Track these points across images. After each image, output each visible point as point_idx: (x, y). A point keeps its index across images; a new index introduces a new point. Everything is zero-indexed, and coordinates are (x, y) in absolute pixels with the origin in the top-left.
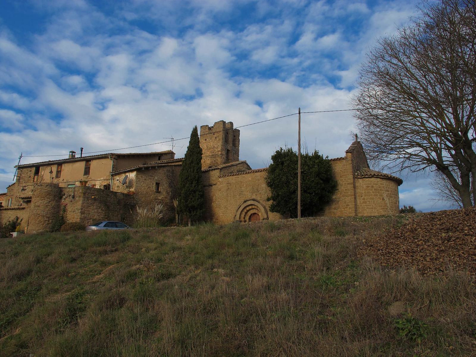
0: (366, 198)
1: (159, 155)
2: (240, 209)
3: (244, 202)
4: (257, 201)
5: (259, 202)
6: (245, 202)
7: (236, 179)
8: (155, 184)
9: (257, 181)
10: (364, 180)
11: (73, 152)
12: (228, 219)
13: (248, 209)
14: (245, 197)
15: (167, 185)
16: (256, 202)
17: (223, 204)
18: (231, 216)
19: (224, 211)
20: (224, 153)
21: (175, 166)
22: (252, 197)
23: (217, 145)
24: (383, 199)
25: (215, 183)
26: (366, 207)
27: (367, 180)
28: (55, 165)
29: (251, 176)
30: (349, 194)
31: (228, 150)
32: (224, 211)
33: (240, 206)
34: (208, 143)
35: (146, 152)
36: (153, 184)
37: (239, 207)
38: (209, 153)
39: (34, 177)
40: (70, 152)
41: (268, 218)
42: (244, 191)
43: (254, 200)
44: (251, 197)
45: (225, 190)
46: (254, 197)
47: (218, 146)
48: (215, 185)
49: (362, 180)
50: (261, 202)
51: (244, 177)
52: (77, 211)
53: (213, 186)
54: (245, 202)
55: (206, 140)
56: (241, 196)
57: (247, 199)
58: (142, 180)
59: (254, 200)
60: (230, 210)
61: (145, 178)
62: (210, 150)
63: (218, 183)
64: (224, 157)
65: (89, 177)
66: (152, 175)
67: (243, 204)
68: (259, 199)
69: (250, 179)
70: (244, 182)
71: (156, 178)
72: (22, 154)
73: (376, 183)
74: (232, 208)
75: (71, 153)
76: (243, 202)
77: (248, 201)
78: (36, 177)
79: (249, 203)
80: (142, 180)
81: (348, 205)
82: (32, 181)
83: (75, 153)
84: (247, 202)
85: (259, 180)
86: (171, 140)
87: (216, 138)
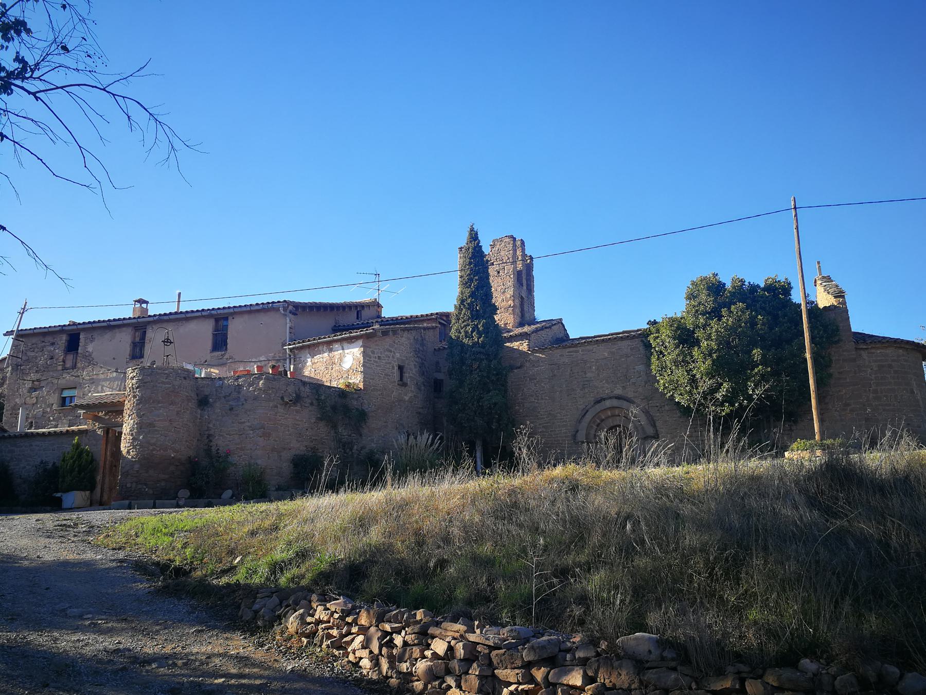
0: (879, 390)
1: (358, 308)
2: (587, 416)
3: (595, 403)
4: (625, 400)
6: (598, 402)
7: (571, 355)
8: (396, 368)
9: (623, 359)
10: (871, 353)
11: (141, 301)
12: (559, 439)
14: (596, 391)
15: (417, 369)
16: (625, 402)
17: (543, 409)
18: (566, 433)
19: (545, 423)
20: (517, 302)
21: (425, 329)
22: (615, 392)
24: (912, 392)
25: (519, 365)
26: (880, 407)
27: (879, 352)
28: (124, 329)
29: (608, 348)
30: (848, 380)
31: (522, 298)
32: (545, 423)
33: (587, 411)
35: (330, 301)
36: (393, 367)
37: (586, 413)
39: (65, 357)
40: (135, 301)
41: (658, 435)
42: (592, 379)
43: (619, 398)
44: (612, 392)
45: (546, 378)
46: (618, 391)
48: (519, 368)
49: (869, 353)
52: (251, 432)
53: (515, 371)
54: (598, 402)
56: (587, 391)
57: (602, 396)
58: (374, 359)
59: (619, 398)
60: (561, 419)
61: (380, 355)
63: (528, 364)
64: (518, 310)
66: (390, 349)
67: (592, 406)
68: (630, 395)
69: (606, 354)
70: (593, 360)
71: (398, 355)
72: (26, 303)
73: (895, 358)
74: (567, 415)
75: (138, 305)
76: (592, 404)
77: (604, 399)
78: (70, 357)
79: (608, 403)
80: (374, 359)
81: (848, 405)
82: (60, 368)
83: (147, 302)
84: (603, 402)
85: (627, 356)
86: (373, 278)
87: (499, 272)
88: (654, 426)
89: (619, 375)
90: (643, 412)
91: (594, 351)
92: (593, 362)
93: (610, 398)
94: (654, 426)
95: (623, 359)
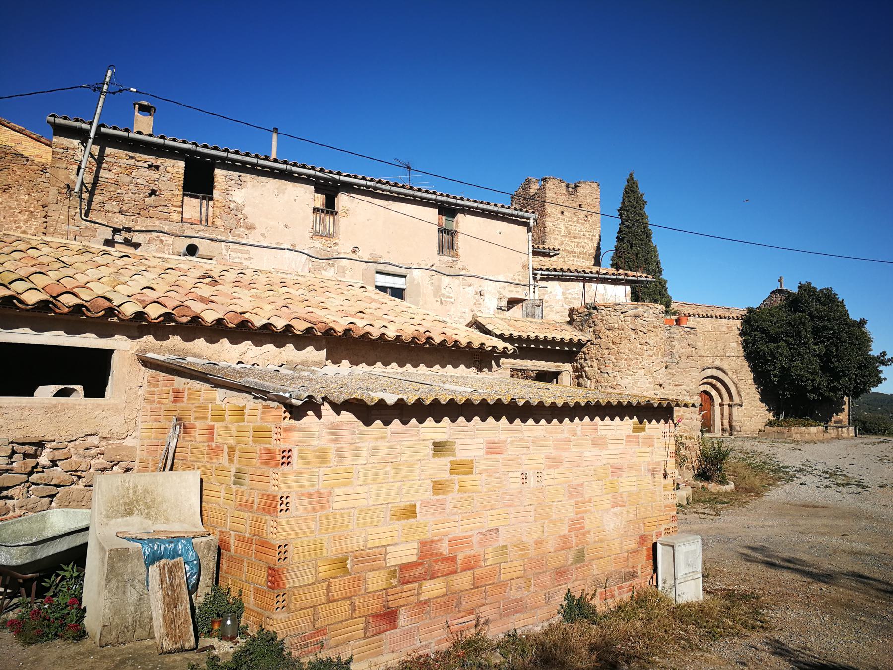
5: (727, 374)
9: (722, 335)
13: (719, 385)
16: (722, 373)
23: (592, 234)
34: (570, 223)
38: (573, 244)
43: (718, 368)
46: (718, 363)
47: (593, 236)
50: (730, 373)
51: (698, 322)
55: (562, 213)
59: (718, 368)
62: (576, 240)
65: (459, 265)
68: (725, 367)
69: (710, 328)
77: (708, 368)
87: (587, 217)
88: (740, 395)
89: (719, 349)
90: (734, 383)
91: (702, 322)
92: (701, 333)
93: (713, 368)
94: (740, 395)
95: (722, 335)
